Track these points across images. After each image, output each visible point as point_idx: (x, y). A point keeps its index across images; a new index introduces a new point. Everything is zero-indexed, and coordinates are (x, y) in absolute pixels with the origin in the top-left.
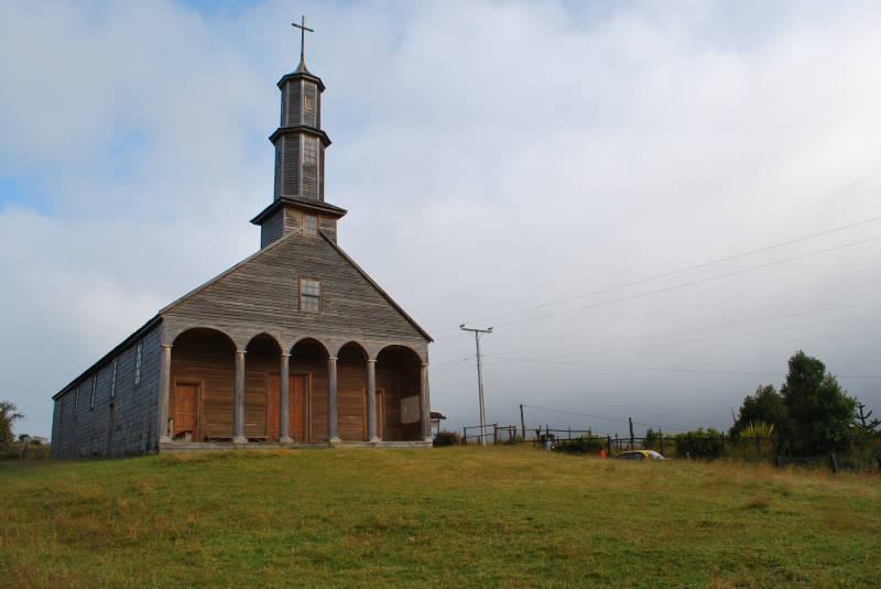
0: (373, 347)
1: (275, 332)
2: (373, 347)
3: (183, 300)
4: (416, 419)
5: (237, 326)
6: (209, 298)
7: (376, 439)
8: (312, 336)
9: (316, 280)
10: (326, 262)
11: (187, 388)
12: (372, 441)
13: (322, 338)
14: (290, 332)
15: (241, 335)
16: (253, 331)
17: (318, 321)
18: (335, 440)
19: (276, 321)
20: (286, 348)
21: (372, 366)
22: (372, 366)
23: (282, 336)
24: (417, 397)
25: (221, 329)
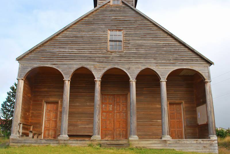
0: (164, 72)
1: (90, 66)
2: (164, 72)
3: (31, 51)
4: (205, 122)
5: (64, 65)
6: (48, 49)
7: (167, 137)
8: (116, 67)
9: (120, 30)
10: (127, 19)
11: (53, 105)
12: (163, 139)
13: (124, 68)
14: (101, 65)
15: (67, 70)
16: (75, 65)
17: (121, 56)
18: (134, 138)
19: (90, 59)
20: (98, 76)
21: (164, 85)
22: (164, 85)
23: (95, 68)
24: (205, 105)
25: (54, 66)
